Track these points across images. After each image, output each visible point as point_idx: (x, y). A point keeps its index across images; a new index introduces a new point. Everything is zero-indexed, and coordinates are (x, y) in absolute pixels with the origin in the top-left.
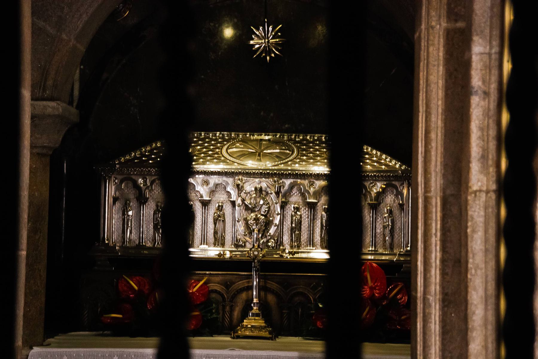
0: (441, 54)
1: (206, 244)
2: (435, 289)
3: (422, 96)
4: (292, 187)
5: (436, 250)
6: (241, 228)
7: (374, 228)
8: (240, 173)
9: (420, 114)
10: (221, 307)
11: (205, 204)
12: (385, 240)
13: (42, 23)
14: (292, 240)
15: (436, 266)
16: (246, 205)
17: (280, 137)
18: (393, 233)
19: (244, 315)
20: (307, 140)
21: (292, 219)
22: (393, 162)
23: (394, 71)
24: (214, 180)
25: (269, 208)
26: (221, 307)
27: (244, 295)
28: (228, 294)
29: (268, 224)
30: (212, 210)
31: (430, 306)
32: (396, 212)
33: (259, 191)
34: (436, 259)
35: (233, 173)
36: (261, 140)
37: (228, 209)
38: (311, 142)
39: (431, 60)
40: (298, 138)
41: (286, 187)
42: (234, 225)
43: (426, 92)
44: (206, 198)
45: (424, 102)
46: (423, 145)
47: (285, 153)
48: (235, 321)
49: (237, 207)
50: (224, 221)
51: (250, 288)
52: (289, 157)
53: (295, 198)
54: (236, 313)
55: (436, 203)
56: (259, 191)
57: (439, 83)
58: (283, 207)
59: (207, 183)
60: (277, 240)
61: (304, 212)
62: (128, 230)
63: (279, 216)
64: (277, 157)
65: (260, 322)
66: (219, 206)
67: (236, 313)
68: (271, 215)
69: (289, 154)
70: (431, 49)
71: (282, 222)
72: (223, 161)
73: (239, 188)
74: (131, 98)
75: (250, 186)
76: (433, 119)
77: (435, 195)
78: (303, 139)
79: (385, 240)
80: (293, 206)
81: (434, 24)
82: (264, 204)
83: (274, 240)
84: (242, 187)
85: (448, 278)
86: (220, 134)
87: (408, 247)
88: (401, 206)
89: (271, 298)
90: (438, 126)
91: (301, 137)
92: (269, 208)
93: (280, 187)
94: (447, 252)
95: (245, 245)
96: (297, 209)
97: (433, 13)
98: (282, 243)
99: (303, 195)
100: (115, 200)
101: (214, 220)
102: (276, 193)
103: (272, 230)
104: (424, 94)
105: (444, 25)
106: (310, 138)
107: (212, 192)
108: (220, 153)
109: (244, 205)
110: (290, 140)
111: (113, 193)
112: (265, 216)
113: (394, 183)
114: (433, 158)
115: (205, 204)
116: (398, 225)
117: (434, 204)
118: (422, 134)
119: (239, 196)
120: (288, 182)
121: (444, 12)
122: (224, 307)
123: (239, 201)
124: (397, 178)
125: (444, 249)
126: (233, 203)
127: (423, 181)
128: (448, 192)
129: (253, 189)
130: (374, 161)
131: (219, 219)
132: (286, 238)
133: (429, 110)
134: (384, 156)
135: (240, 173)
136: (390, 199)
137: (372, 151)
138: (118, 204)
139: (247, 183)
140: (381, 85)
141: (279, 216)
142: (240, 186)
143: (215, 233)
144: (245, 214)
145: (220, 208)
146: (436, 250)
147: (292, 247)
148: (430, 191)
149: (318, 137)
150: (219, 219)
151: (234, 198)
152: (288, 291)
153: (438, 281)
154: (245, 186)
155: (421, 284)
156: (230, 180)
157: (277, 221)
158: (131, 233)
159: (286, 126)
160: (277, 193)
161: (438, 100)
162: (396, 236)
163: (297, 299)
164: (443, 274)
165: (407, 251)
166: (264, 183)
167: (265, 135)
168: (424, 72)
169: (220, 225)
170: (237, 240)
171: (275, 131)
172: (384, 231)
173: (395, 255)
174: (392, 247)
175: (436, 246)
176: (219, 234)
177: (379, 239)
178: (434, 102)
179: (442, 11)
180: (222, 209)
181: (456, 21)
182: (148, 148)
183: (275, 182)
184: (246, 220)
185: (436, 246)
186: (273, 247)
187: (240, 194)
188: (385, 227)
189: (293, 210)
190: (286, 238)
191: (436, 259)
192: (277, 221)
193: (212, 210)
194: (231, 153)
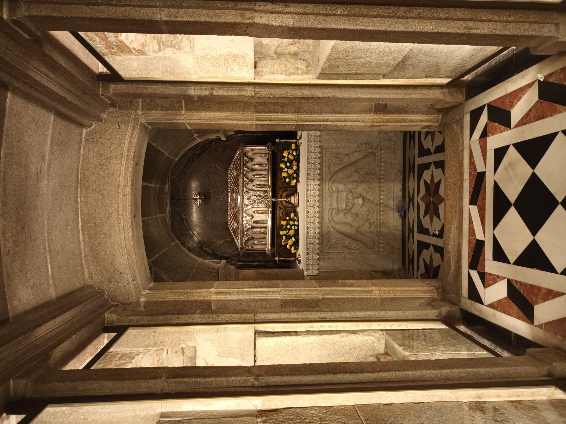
0: (196, 114)
3: (214, 122)
4: (246, 188)
6: (260, 205)
7: (260, 160)
19: (289, 202)
24: (244, 215)
27: (284, 203)
29: (259, 195)
31: (300, 118)
32: (254, 152)
33: (248, 199)
37: (254, 209)
41: (246, 190)
42: (260, 207)
44: (251, 217)
48: (292, 206)
51: (281, 201)
53: (250, 186)
54: (289, 205)
56: (248, 199)
58: (254, 191)
59: (246, 217)
61: (255, 183)
65: (293, 198)
67: (289, 205)
71: (258, 191)
73: (247, 206)
75: (246, 202)
76: (223, 117)
81: (183, 117)
85: (289, 111)
88: (252, 150)
89: (285, 194)
94: (278, 111)
96: (254, 186)
97: (179, 118)
100: (252, 247)
103: (261, 194)
105: (184, 112)
107: (248, 215)
110: (230, 190)
115: (253, 217)
116: (258, 151)
119: (250, 206)
120: (245, 189)
121: (178, 113)
122: (287, 210)
123: (251, 205)
125: (277, 112)
126: (252, 207)
128: (254, 110)
131: (257, 212)
132: (264, 189)
136: (250, 154)
138: (253, 246)
143: (262, 213)
144: (256, 204)
145: (254, 212)
150: (257, 212)
153: (290, 115)
156: (245, 209)
157: (258, 193)
160: (249, 192)
164: (287, 113)
166: (246, 197)
169: (260, 212)
171: (227, 195)
179: (178, 113)
181: (182, 107)
188: (259, 156)
192: (258, 193)
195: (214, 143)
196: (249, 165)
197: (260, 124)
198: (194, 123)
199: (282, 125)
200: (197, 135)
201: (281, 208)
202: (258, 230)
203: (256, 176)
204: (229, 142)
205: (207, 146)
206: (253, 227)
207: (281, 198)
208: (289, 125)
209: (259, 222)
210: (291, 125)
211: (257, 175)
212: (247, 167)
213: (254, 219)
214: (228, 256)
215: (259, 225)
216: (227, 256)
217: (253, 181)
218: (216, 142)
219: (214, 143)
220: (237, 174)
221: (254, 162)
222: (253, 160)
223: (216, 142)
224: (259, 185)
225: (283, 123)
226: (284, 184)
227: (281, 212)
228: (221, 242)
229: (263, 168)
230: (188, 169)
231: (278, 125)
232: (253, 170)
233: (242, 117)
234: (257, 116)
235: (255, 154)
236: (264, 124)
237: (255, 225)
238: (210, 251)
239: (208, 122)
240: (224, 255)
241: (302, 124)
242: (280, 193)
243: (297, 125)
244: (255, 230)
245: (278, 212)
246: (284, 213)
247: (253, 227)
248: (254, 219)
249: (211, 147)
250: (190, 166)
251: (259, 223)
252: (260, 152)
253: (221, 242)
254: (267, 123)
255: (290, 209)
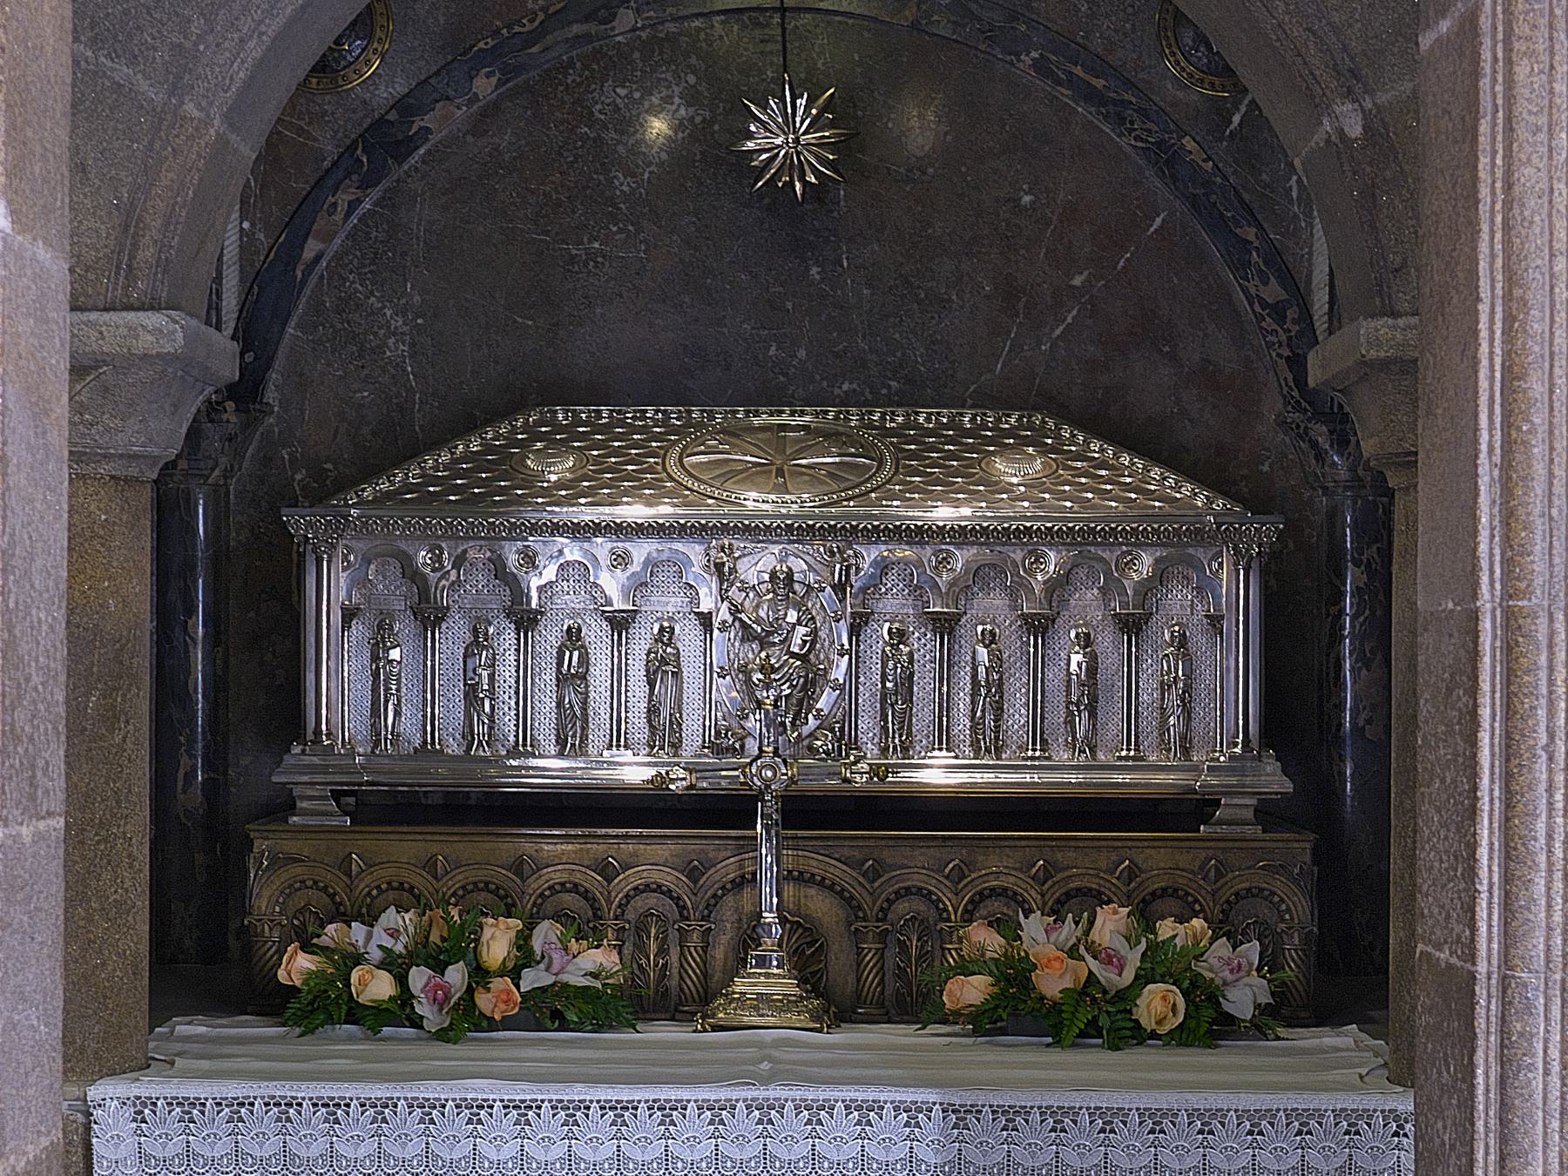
1: (626, 747)
2: (1548, 949)
3: (1488, 246)
4: (883, 567)
5: (1551, 804)
6: (726, 691)
8: (725, 529)
9: (1484, 309)
10: (673, 936)
11: (620, 623)
12: (1163, 726)
13: (124, 68)
14: (885, 728)
15: (1550, 864)
16: (744, 625)
17: (836, 418)
18: (1190, 702)
20: (918, 427)
21: (884, 666)
22: (1187, 489)
23: (1159, 220)
24: (641, 551)
25: (814, 633)
26: (673, 936)
28: (695, 895)
29: (811, 684)
30: (641, 641)
32: (1199, 640)
33: (783, 582)
34: (1550, 837)
35: (704, 527)
36: (783, 427)
37: (688, 637)
38: (931, 432)
39: (1522, 108)
40: (892, 420)
42: (707, 689)
43: (1507, 227)
44: (618, 604)
45: (1499, 262)
46: (1498, 420)
47: (856, 466)
49: (716, 632)
50: (677, 675)
52: (867, 481)
53: (893, 603)
55: (1552, 634)
57: (1556, 194)
58: (854, 631)
59: (621, 560)
60: (842, 729)
61: (922, 644)
62: (390, 707)
63: (847, 657)
64: (831, 475)
66: (662, 629)
68: (822, 656)
69: (869, 467)
70: (1522, 70)
71: (854, 672)
72: (670, 494)
73: (722, 573)
74: (389, 313)
75: (757, 565)
77: (1546, 603)
78: (906, 426)
79: (1163, 726)
80: (887, 625)
82: (799, 622)
83: (832, 730)
84: (733, 570)
86: (657, 412)
87: (1236, 744)
88: (1215, 621)
89: (821, 906)
90: (1556, 349)
91: (900, 419)
92: (814, 633)
93: (848, 568)
95: (742, 747)
96: (900, 636)
98: (854, 744)
99: (917, 591)
100: (349, 615)
101: (648, 671)
102: (833, 587)
103: (825, 701)
104: (1498, 236)
106: (928, 420)
107: (638, 586)
108: (659, 467)
109: (737, 624)
111: (343, 594)
112: (803, 658)
113: (1191, 551)
114: (1540, 469)
115: (620, 623)
116: (1206, 677)
117: (1542, 637)
118: (1492, 378)
120: (870, 555)
123: (724, 614)
124: (1199, 536)
126: (706, 620)
127: (1497, 551)
129: (766, 577)
130: (1128, 488)
131: (663, 666)
132: (867, 726)
133: (1517, 292)
134: (1156, 473)
135: (725, 529)
136: (1178, 600)
137: (1116, 456)
138: (358, 629)
139: (745, 559)
140: (1121, 264)
141: (847, 657)
142: (726, 569)
143: (652, 711)
145: (666, 635)
146: (1551, 804)
147: (884, 751)
148: (1527, 593)
149: (952, 418)
150: (663, 666)
151: (706, 605)
152: (877, 884)
154: (741, 566)
155: (1490, 926)
156: (694, 552)
157: (839, 672)
158: (397, 713)
159: (845, 387)
160: (839, 588)
161: (1552, 255)
162: (1198, 711)
163: (902, 907)
165: (1232, 758)
167: (792, 414)
168: (1494, 152)
170: (718, 733)
171: (818, 400)
172: (1163, 699)
173: (1196, 769)
174: (1186, 752)
175: (1550, 789)
176: (665, 713)
177: (1150, 721)
178: (1539, 262)
180: (670, 639)
182: (445, 458)
183: (832, 554)
184: (744, 670)
185: (1550, 789)
186: (827, 753)
187: (727, 591)
188: (1164, 687)
189: (887, 638)
190: (867, 726)
191: (1550, 837)
192: (839, 672)
193: (641, 641)
194: (694, 465)
195: (1273, 291)
196: (1087, 602)
197: (1475, 655)
198: (1476, 75)
199: (1473, 847)
200: (1355, 129)
201: (694, 874)
202: (506, 673)
203: (983, 653)
204: (1282, 423)
205: (1251, 233)
206: (526, 621)
207: (785, 877)
208: (1471, 910)
209: (572, 679)
210: (1473, 929)
211: (997, 658)
212: (1059, 586)
213: (596, 635)
214: (267, 410)
215: (549, 676)
216: (271, 395)
217: (945, 626)
218: (1278, 312)
219: (1273, 291)
220: (1008, 489)
221: (1106, 641)
222: (1132, 626)
223: (1278, 312)
224: (907, 682)
225: (1483, 853)
226: (920, 906)
227: (668, 878)
228: (396, 349)
229: (1057, 716)
230: (1040, 66)
231: (1473, 812)
232: (1039, 626)
233: (1539, 488)
234: (1543, 621)
235: (1182, 642)
236: (1474, 690)
237: (549, 637)
238: (311, 248)
239: (1484, 192)
240: (274, 374)
241: (1480, 1024)
242: (837, 871)
243: (1473, 977)
244: (506, 639)
245: (664, 851)
246: (652, 900)
247: (526, 621)
248: (596, 635)
249: (1241, 267)
250: (1072, 81)
251: (562, 680)
252: (1201, 688)
253: (396, 349)
254: (1485, 713)
255: (695, 956)
